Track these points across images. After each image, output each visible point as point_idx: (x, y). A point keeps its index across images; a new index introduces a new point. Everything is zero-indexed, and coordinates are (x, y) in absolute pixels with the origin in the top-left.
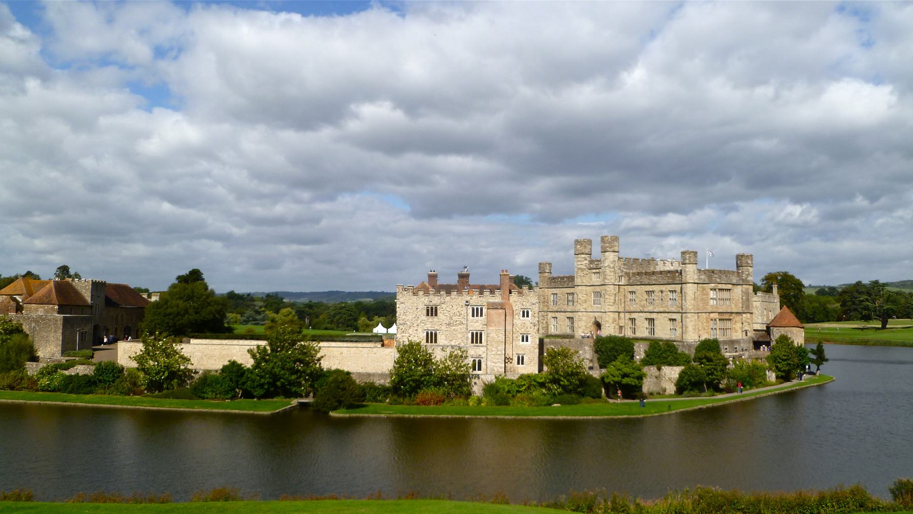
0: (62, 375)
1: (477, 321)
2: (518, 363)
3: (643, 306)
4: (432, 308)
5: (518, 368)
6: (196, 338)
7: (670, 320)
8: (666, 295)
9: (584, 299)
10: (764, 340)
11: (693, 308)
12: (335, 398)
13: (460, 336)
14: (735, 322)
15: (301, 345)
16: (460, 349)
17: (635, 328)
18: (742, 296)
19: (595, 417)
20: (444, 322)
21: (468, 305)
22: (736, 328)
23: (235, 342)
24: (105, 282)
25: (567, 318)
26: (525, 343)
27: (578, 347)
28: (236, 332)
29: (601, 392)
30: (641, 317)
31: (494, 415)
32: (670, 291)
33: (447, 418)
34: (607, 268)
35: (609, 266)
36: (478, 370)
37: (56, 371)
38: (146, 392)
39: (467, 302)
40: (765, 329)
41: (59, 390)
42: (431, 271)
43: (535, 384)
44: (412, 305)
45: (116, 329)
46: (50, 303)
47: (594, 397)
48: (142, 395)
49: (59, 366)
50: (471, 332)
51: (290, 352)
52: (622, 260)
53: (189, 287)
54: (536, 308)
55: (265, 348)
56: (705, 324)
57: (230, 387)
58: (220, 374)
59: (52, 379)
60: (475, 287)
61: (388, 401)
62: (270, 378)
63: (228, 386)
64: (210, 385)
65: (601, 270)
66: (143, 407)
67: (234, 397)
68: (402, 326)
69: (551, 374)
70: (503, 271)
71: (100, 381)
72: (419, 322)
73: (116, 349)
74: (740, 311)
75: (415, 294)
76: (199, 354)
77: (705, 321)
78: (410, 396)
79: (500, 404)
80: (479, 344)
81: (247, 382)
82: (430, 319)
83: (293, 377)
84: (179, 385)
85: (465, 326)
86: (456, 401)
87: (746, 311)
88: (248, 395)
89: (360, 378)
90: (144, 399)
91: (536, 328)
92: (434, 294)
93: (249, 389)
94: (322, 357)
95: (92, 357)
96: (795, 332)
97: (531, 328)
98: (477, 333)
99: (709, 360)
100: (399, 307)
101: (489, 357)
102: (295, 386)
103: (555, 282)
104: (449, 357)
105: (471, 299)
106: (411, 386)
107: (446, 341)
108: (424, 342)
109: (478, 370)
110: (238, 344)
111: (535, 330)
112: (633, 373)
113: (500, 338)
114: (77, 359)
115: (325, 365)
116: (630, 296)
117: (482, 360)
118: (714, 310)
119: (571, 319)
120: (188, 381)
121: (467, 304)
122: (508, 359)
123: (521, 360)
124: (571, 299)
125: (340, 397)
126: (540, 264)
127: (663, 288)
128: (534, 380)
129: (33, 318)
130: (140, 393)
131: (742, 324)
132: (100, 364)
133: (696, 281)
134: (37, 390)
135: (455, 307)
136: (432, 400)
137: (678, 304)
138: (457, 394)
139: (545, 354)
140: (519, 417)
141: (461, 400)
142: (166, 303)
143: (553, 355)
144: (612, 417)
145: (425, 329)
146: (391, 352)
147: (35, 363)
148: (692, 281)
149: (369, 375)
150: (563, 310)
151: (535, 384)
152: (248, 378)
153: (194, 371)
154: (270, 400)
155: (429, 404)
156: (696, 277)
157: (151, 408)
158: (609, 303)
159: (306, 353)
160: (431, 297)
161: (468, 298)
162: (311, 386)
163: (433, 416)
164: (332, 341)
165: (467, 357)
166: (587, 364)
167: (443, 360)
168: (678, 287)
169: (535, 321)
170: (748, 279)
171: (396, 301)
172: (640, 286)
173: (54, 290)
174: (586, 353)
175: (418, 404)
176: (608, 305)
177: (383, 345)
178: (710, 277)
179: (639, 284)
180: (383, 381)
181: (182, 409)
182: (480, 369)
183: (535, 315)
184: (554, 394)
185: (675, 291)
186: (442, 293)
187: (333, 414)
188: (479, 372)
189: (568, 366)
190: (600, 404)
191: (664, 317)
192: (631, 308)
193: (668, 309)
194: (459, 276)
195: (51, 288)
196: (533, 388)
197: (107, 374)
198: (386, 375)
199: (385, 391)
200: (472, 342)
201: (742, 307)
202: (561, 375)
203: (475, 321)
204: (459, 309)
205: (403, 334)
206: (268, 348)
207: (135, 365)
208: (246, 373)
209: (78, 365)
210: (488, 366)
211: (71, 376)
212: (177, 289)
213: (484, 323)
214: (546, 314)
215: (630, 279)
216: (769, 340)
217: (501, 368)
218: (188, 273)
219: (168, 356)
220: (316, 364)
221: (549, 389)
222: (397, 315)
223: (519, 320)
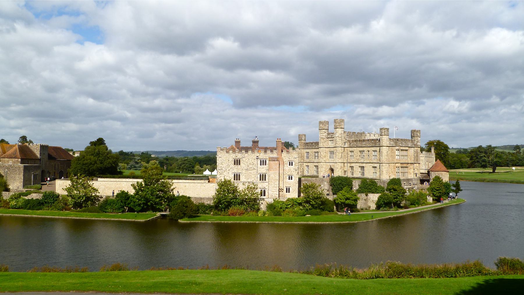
0: (24, 199)
1: (263, 168)
2: (287, 192)
3: (358, 159)
4: (237, 160)
6: (101, 177)
7: (373, 167)
8: (371, 153)
9: (325, 155)
10: (426, 179)
11: (386, 161)
12: (181, 212)
13: (253, 176)
14: (410, 169)
15: (162, 181)
16: (253, 184)
18: (414, 154)
19: (330, 223)
21: (258, 159)
22: (410, 172)
23: (124, 180)
24: (48, 145)
25: (315, 166)
26: (290, 180)
28: (124, 174)
29: (334, 208)
30: (356, 165)
31: (272, 221)
32: (373, 151)
34: (338, 138)
35: (338, 137)
36: (264, 196)
37: (20, 197)
38: (72, 209)
39: (257, 157)
40: (427, 173)
41: (22, 208)
42: (237, 139)
43: (296, 203)
44: (226, 158)
45: (55, 173)
47: (329, 211)
48: (70, 211)
49: (21, 194)
50: (259, 174)
51: (156, 186)
52: (346, 133)
53: (97, 148)
54: (297, 160)
55: (141, 183)
56: (393, 170)
57: (121, 206)
58: (115, 198)
59: (18, 202)
60: (262, 148)
61: (212, 213)
62: (144, 200)
63: (120, 205)
64: (110, 204)
65: (334, 139)
66: (71, 218)
67: (123, 211)
69: (305, 198)
70: (278, 139)
71: (46, 203)
73: (55, 184)
74: (413, 162)
76: (103, 187)
77: (393, 168)
78: (225, 211)
79: (276, 215)
80: (264, 181)
81: (131, 203)
82: (236, 166)
83: (158, 200)
84: (92, 205)
85: (256, 171)
86: (251, 213)
87: (416, 162)
88: (131, 210)
89: (196, 200)
90: (72, 213)
92: (238, 152)
93: (132, 207)
94: (174, 188)
95: (41, 189)
97: (294, 172)
98: (263, 175)
99: (395, 190)
102: (158, 205)
103: (308, 145)
104: (247, 188)
105: (259, 155)
106: (225, 205)
107: (245, 180)
108: (232, 180)
109: (264, 196)
110: (125, 181)
112: (352, 198)
113: (276, 178)
114: (32, 190)
116: (350, 154)
118: (398, 162)
120: (97, 203)
121: (257, 158)
122: (281, 189)
123: (288, 190)
125: (184, 211)
126: (412, 131)
127: (369, 149)
128: (295, 201)
129: (6, 166)
130: (69, 209)
131: (414, 169)
132: (46, 193)
133: (388, 145)
134: (9, 208)
135: (250, 160)
136: (237, 213)
137: (378, 158)
138: (251, 210)
139: (302, 187)
140: (287, 223)
141: (254, 213)
142: (84, 157)
143: (307, 187)
144: (340, 222)
145: (234, 172)
148: (386, 145)
149: (201, 199)
150: (312, 162)
151: (296, 203)
152: (132, 200)
153: (100, 197)
154: (144, 213)
155: (236, 215)
156: (388, 143)
157: (75, 218)
158: (338, 158)
159: (165, 186)
160: (237, 154)
161: (258, 155)
162: (168, 205)
165: (257, 188)
166: (326, 192)
168: (378, 149)
169: (296, 168)
170: (418, 144)
171: (216, 156)
172: (356, 148)
173: (18, 150)
174: (325, 186)
175: (229, 215)
176: (338, 159)
177: (209, 182)
178: (396, 143)
180: (209, 202)
181: (93, 219)
182: (264, 195)
183: (296, 164)
184: (307, 209)
186: (243, 151)
187: (180, 221)
189: (315, 193)
190: (333, 215)
191: (370, 166)
192: (351, 161)
193: (372, 161)
195: (17, 149)
196: (295, 206)
197: (49, 198)
198: (211, 199)
199: (210, 208)
200: (260, 180)
201: (414, 160)
202: (311, 199)
204: (253, 161)
206: (143, 183)
207: (66, 193)
208: (130, 198)
209: (33, 194)
210: (269, 193)
211: (29, 200)
212: (90, 150)
214: (302, 164)
215: (350, 144)
216: (429, 179)
217: (277, 194)
218: (96, 140)
219: (85, 188)
220: (170, 192)
221: (304, 206)
222: (217, 164)
223: (287, 167)
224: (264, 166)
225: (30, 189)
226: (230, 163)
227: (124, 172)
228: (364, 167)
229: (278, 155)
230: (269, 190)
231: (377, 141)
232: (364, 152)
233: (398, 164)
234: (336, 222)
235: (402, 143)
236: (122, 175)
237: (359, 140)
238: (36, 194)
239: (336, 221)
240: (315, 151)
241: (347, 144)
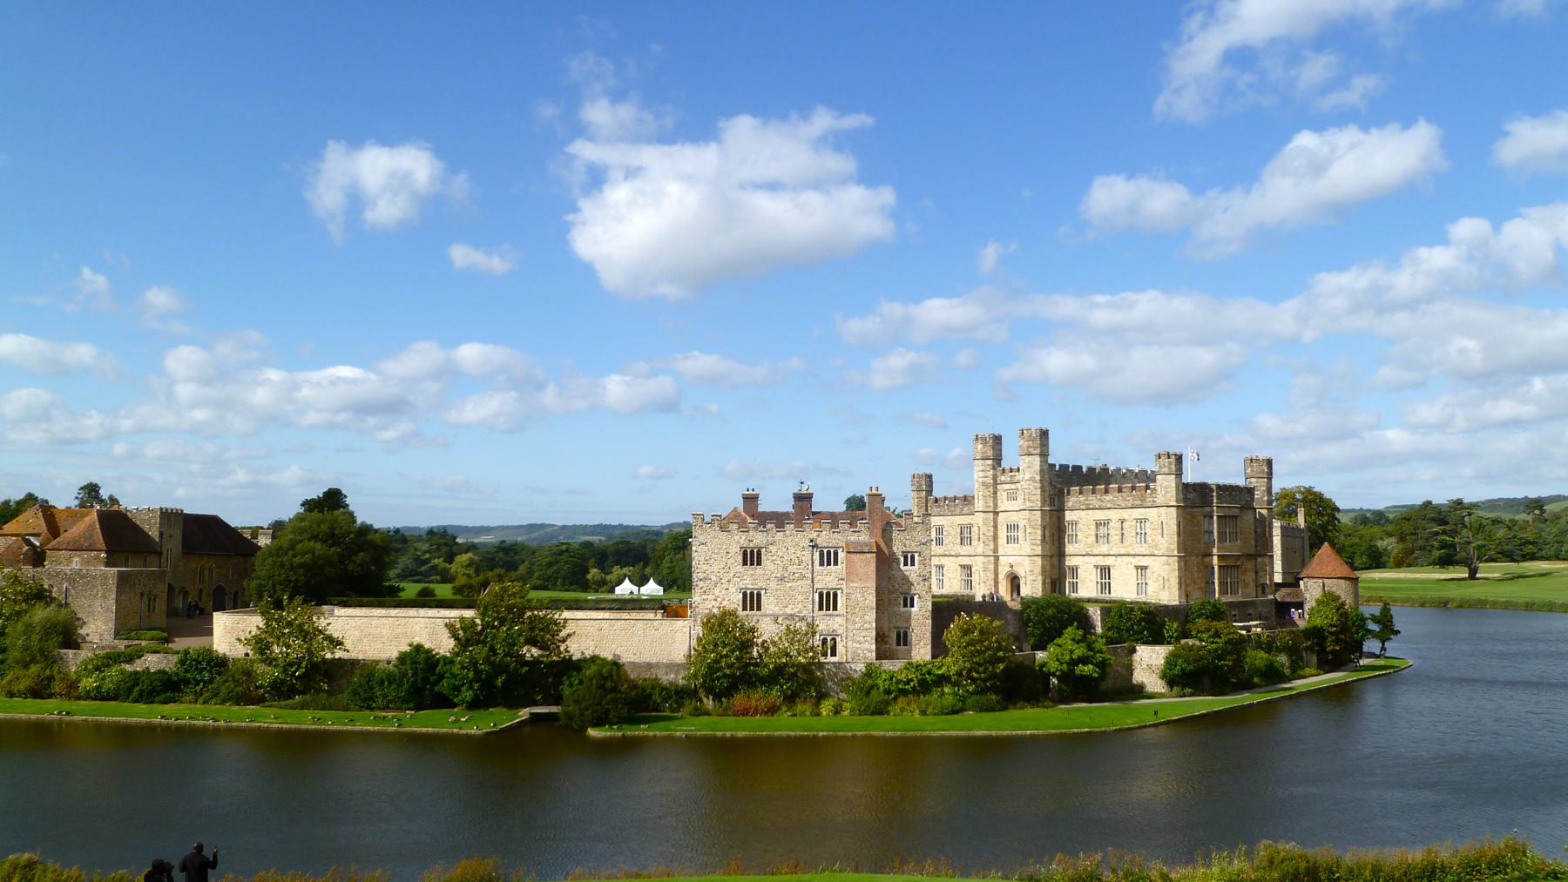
0: (122, 672)
1: (829, 574)
2: (898, 644)
4: (752, 552)
5: (897, 651)
8: (1131, 526)
10: (1293, 600)
13: (800, 598)
14: (1245, 571)
20: (774, 575)
22: (1247, 581)
23: (412, 612)
24: (182, 511)
25: (961, 566)
33: (789, 736)
36: (831, 656)
41: (114, 698)
45: (201, 591)
46: (91, 548)
49: (113, 658)
56: (1196, 575)
58: (395, 666)
59: (103, 679)
68: (702, 582)
71: (187, 682)
72: (731, 575)
75: (723, 528)
77: (1196, 569)
85: (810, 582)
92: (756, 529)
97: (918, 584)
98: (828, 594)
99: (1217, 635)
105: (818, 536)
109: (831, 656)
114: (144, 643)
115: (577, 648)
117: (838, 639)
119: (967, 569)
127: (1125, 514)
129: (66, 574)
134: (79, 698)
145: (741, 586)
146: (684, 627)
147: (71, 651)
149: (649, 666)
150: (953, 553)
158: (1034, 541)
163: (764, 733)
164: (577, 609)
167: (776, 639)
168: (1151, 513)
171: (690, 540)
173: (98, 527)
174: (1008, 625)
179: (1083, 507)
182: (834, 654)
185: (1146, 520)
188: (833, 659)
198: (679, 665)
200: (821, 609)
201: (1256, 546)
203: (825, 572)
205: (703, 596)
206: (478, 621)
208: (441, 664)
210: (850, 650)
211: (136, 673)
216: (1301, 600)
218: (321, 496)
222: (693, 563)
224: (832, 567)
225: (137, 642)
226: (732, 560)
227: (403, 589)
234: (1053, 731)
236: (397, 596)
238: (158, 655)
239: (1054, 729)
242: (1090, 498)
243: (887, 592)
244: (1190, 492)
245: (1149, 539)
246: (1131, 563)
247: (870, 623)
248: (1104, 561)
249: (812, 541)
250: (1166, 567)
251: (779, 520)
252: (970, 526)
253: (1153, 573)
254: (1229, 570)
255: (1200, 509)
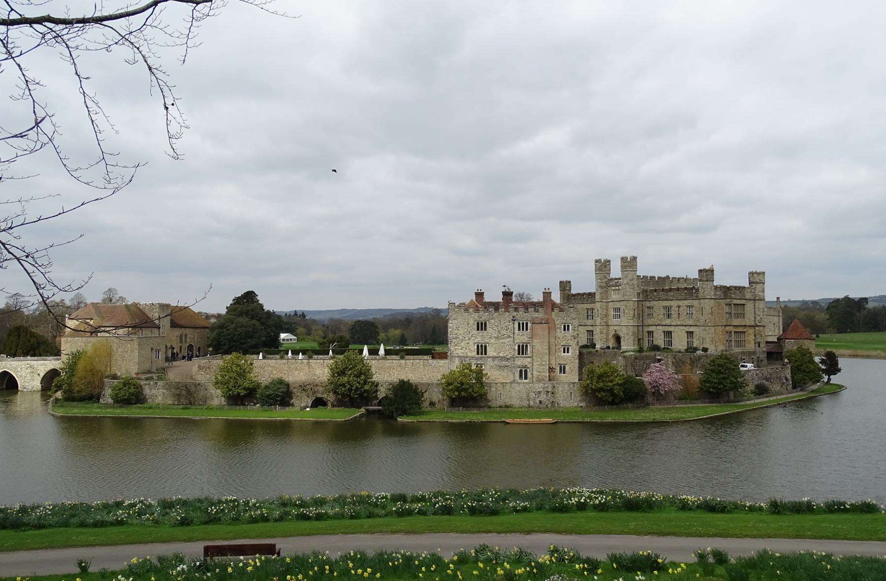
1: (523, 335)
2: (561, 372)
3: (661, 320)
4: (482, 323)
7: (687, 332)
9: (605, 314)
11: (710, 322)
17: (653, 340)
20: (493, 336)
21: (515, 320)
22: (749, 340)
25: (587, 331)
26: (566, 354)
27: (612, 357)
30: (659, 330)
34: (627, 285)
40: (777, 341)
65: (620, 287)
75: (466, 310)
77: (721, 333)
85: (512, 339)
91: (576, 340)
96: (806, 343)
97: (571, 340)
98: (523, 346)
100: (451, 323)
101: (535, 368)
103: (575, 299)
105: (517, 315)
111: (575, 343)
117: (528, 370)
119: (590, 332)
121: (514, 319)
122: (551, 369)
123: (563, 370)
124: (590, 314)
127: (681, 303)
133: (713, 297)
137: (695, 318)
145: (477, 342)
148: (710, 297)
150: (583, 324)
156: (713, 293)
160: (481, 313)
168: (696, 303)
185: (692, 306)
191: (682, 330)
194: (503, 294)
200: (519, 354)
203: (521, 334)
210: (534, 375)
213: (529, 336)
216: (781, 351)
223: (560, 333)
224: (525, 332)
228: (671, 332)
229: (546, 313)
230: (534, 370)
231: (694, 291)
232: (671, 308)
233: (730, 327)
235: (735, 293)
237: (663, 289)
240: (587, 307)
241: (643, 296)
242: (660, 294)
243: (554, 345)
244: (718, 291)
245: (694, 317)
246: (684, 330)
247: (545, 361)
248: (668, 329)
249: (514, 317)
250: (704, 332)
251: (496, 306)
252: (592, 309)
253: (697, 335)
254: (739, 334)
255: (724, 300)
